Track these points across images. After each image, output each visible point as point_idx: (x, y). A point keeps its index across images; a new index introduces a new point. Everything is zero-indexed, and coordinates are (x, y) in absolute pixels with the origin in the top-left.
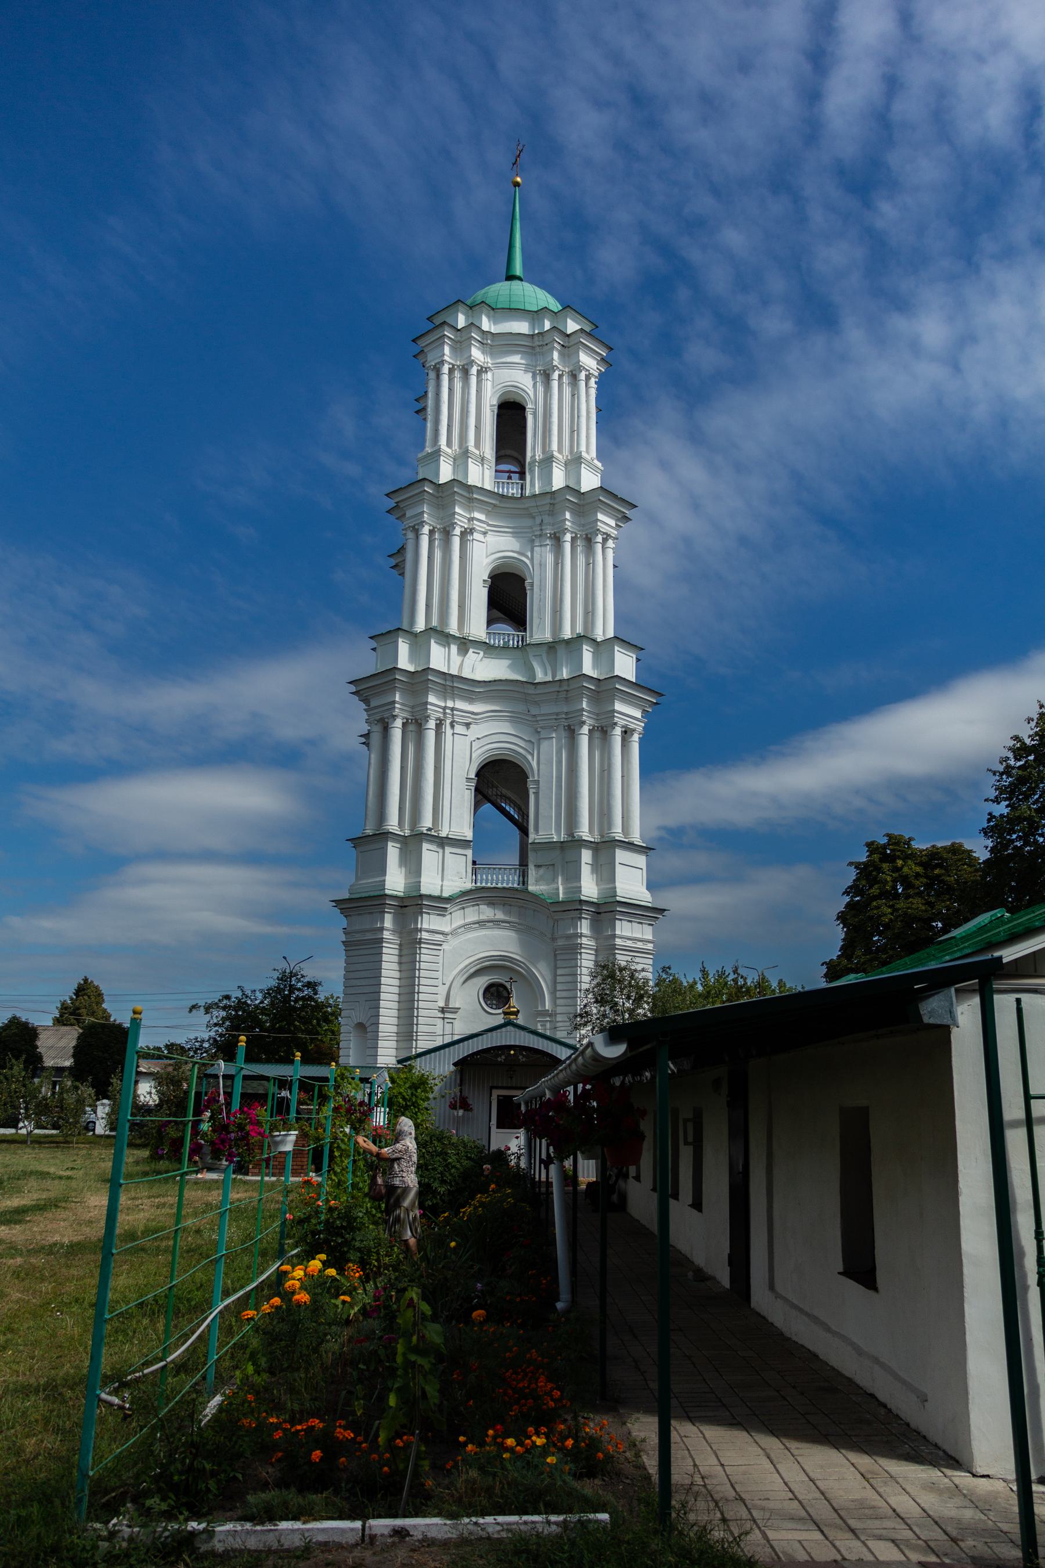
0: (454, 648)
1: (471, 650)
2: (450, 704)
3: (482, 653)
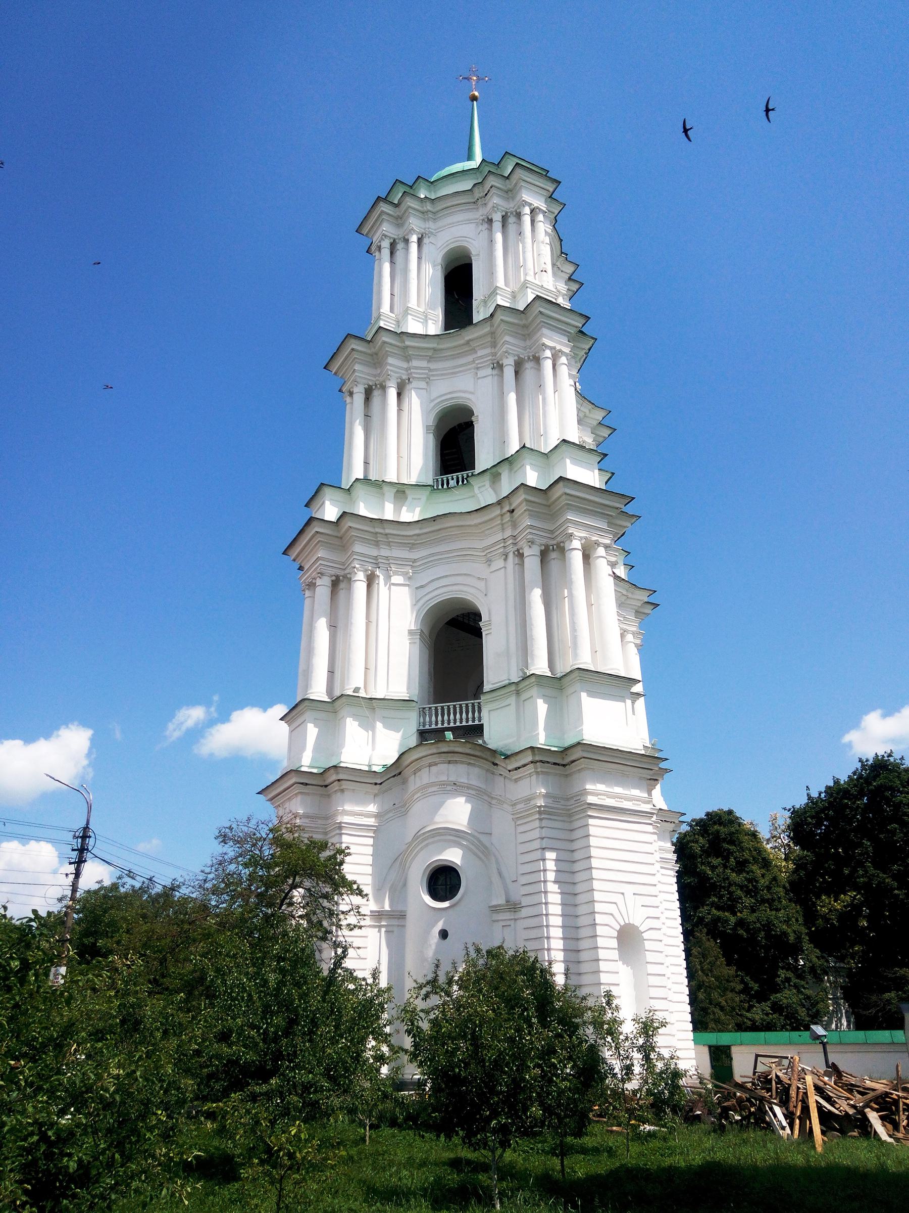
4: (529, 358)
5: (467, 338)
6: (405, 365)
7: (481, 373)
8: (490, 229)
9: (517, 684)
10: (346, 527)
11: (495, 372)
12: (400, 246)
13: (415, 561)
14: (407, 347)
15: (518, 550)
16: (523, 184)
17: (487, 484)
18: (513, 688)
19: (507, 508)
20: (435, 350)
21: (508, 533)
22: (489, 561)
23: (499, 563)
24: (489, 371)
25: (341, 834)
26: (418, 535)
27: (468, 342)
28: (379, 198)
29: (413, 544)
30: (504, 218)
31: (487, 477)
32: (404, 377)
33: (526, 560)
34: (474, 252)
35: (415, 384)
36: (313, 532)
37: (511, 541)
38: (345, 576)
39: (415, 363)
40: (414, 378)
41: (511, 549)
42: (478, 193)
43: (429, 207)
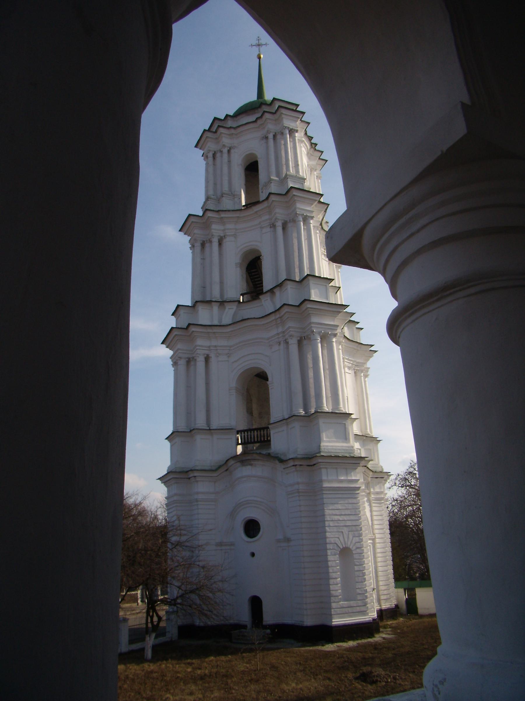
0: (215, 308)
2: (214, 343)
5: (255, 210)
6: (222, 228)
7: (264, 230)
8: (267, 143)
11: (272, 229)
12: (218, 155)
13: (231, 347)
14: (222, 218)
15: (286, 340)
17: (269, 298)
18: (284, 421)
19: (278, 316)
20: (238, 217)
21: (280, 330)
24: (268, 229)
25: (198, 505)
26: (232, 331)
27: (256, 212)
28: (205, 131)
30: (275, 136)
31: (268, 294)
32: (222, 235)
33: (290, 347)
35: (228, 239)
37: (281, 335)
38: (193, 358)
39: (229, 226)
42: (259, 122)
43: (233, 131)
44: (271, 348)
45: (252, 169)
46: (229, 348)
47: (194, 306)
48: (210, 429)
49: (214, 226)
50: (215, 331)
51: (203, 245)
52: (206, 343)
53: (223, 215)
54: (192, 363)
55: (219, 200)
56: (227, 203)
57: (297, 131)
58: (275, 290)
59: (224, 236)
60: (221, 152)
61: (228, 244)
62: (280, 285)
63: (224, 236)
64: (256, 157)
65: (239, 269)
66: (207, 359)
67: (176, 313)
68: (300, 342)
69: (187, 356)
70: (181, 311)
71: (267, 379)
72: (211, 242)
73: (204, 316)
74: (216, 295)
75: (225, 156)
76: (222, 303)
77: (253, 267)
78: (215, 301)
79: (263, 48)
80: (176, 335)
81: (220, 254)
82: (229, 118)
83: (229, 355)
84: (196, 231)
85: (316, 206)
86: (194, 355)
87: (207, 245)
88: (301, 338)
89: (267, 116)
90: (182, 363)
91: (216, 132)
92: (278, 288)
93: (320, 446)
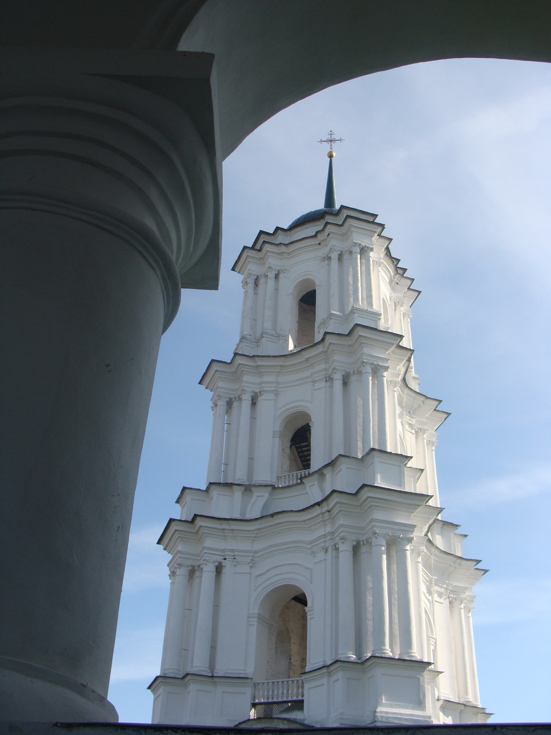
0: (238, 493)
1: (255, 495)
3: (266, 495)
4: (354, 372)
9: (328, 666)
10: (198, 526)
11: (328, 384)
12: (262, 281)
13: (256, 552)
14: (259, 366)
15: (335, 545)
16: (353, 229)
17: (316, 483)
18: (325, 670)
20: (281, 366)
21: (329, 529)
22: (313, 554)
23: (321, 556)
24: (323, 384)
26: (259, 529)
27: (307, 360)
28: (245, 248)
29: (255, 537)
32: (257, 391)
33: (341, 555)
34: (317, 283)
36: (173, 530)
37: (329, 537)
38: (199, 566)
39: (266, 379)
40: (264, 391)
41: (329, 544)
42: (320, 237)
43: (283, 249)
44: (314, 557)
45: (308, 300)
46: (252, 554)
47: (207, 490)
48: (212, 677)
49: (246, 378)
50: (233, 527)
51: (230, 404)
52: (221, 545)
53: (259, 362)
54: (197, 574)
55: (257, 342)
56: (268, 347)
57: (372, 249)
58: (325, 471)
59: (261, 392)
60: (266, 276)
61: (265, 405)
62: (332, 464)
63: (261, 392)
64: (313, 284)
65: (277, 439)
66: (219, 569)
67: (182, 501)
68: (356, 549)
69: (189, 563)
70: (188, 497)
71: (305, 603)
72: (240, 399)
73: (223, 505)
74: (240, 476)
75: (271, 282)
76: (248, 488)
77: (299, 440)
78: (238, 485)
79: (334, 145)
80: (176, 530)
81: (253, 418)
82: (279, 231)
83: (253, 564)
84: (220, 384)
85: (393, 352)
86: (200, 563)
87: (235, 404)
88: (358, 543)
89: (330, 228)
90: (182, 572)
91: (260, 250)
92: (329, 468)
93: (375, 712)
